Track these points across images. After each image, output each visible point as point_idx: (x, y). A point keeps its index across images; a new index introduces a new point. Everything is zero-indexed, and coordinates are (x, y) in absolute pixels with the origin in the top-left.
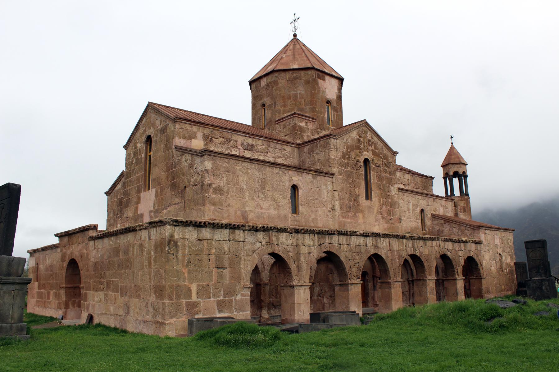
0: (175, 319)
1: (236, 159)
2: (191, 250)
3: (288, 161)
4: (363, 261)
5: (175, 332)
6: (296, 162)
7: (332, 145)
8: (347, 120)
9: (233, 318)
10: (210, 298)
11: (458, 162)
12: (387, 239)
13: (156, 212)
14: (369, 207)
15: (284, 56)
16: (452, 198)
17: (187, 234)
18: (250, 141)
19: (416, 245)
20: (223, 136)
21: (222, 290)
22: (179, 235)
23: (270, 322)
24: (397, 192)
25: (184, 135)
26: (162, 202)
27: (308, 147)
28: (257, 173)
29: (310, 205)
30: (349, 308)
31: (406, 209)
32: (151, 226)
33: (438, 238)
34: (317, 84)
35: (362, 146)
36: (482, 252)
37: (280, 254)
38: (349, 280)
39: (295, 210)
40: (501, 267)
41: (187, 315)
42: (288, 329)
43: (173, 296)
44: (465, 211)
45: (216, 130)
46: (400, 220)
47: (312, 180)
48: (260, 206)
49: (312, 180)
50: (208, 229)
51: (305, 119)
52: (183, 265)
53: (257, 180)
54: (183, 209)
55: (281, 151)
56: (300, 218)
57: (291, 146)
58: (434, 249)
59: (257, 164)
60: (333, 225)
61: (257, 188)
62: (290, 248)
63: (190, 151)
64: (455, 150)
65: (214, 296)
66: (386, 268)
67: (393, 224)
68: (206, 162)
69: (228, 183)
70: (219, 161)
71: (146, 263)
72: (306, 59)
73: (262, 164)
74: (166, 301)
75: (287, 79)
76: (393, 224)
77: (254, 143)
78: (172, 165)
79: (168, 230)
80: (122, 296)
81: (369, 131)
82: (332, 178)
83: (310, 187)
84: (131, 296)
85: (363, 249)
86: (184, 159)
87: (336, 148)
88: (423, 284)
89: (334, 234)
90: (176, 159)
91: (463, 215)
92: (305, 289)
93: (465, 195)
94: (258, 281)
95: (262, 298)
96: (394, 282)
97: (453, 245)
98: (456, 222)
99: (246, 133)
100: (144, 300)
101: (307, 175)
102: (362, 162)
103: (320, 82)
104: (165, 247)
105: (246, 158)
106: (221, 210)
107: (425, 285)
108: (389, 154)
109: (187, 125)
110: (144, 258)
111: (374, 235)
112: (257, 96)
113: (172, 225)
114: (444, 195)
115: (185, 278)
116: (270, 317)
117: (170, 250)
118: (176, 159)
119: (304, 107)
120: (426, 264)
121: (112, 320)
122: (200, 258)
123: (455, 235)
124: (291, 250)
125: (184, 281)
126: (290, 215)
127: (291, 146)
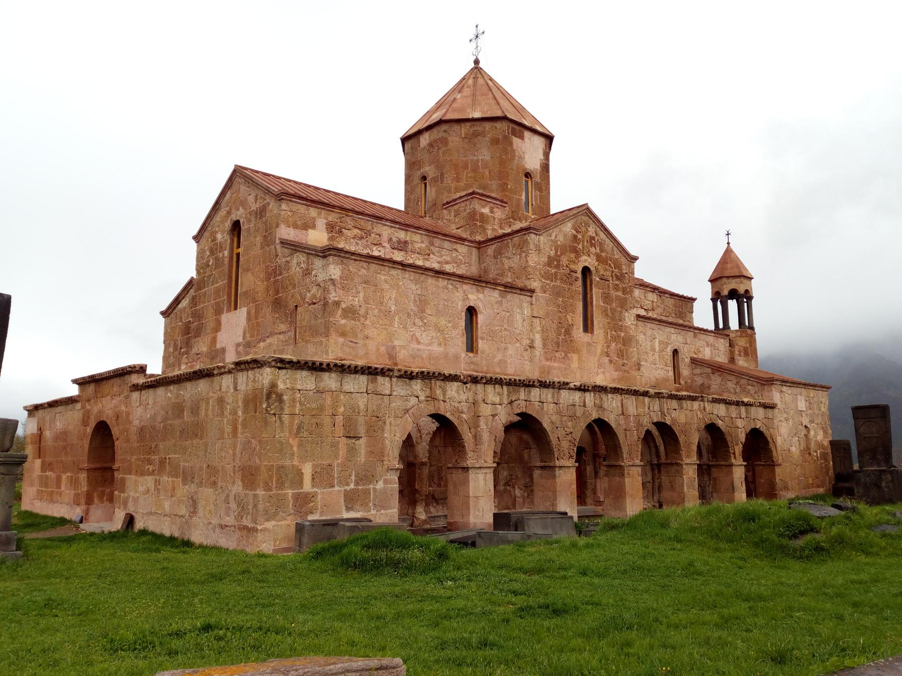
0: (273, 523)
1: (380, 263)
2: (304, 407)
3: (461, 268)
4: (578, 430)
5: (272, 544)
6: (474, 270)
7: (531, 243)
8: (558, 202)
9: (370, 521)
10: (333, 486)
11: (738, 275)
12: (619, 396)
13: (248, 345)
14: (589, 344)
15: (459, 96)
16: (726, 332)
17: (299, 382)
18: (402, 235)
19: (666, 407)
20: (359, 226)
21: (354, 473)
22: (285, 383)
23: (429, 526)
24: (634, 321)
25: (296, 221)
26: (258, 330)
27: (494, 247)
28: (413, 287)
29: (495, 339)
30: (556, 505)
31: (649, 348)
32: (238, 368)
33: (702, 397)
34: (511, 144)
35: (580, 246)
36: (775, 421)
37: (448, 415)
38: (557, 461)
39: (471, 346)
40: (808, 448)
41: (295, 515)
42: (458, 539)
43: (272, 484)
44: (746, 354)
45: (347, 215)
46: (638, 367)
47: (500, 299)
48: (417, 339)
49: (500, 299)
50: (333, 375)
52: (290, 432)
54: (291, 341)
55: (451, 252)
56: (479, 359)
57: (467, 245)
58: (695, 415)
59: (414, 272)
60: (530, 372)
61: (412, 309)
62: (464, 407)
63: (305, 248)
64: (732, 254)
65: (340, 483)
66: (616, 443)
67: (628, 372)
68: (332, 266)
70: (353, 266)
71: (228, 429)
72: (492, 101)
73: (421, 272)
74: (260, 492)
75: (463, 136)
76: (628, 372)
77: (408, 239)
78: (274, 271)
79: (267, 375)
80: (184, 484)
82: (531, 297)
83: (496, 310)
84: (200, 484)
85: (579, 412)
86: (295, 261)
87: (538, 250)
88: (678, 471)
89: (533, 386)
90: (281, 261)
91: (744, 360)
92: (486, 473)
93: (747, 327)
94: (411, 459)
95: (417, 487)
96: (629, 466)
97: (727, 409)
98: (731, 371)
99: (396, 223)
100: (223, 491)
102: (578, 272)
103: (516, 141)
104: (261, 403)
105: (395, 262)
106: (355, 345)
107: (680, 473)
108: (623, 260)
109: (300, 206)
110: (225, 420)
112: (414, 163)
113: (274, 367)
114: (711, 327)
115: (293, 454)
116: (429, 517)
117: (270, 407)
118: (281, 261)
119: (489, 182)
120: (682, 439)
121: (166, 523)
122: (319, 421)
123: (730, 392)
124: (465, 410)
125: (292, 458)
126: (463, 355)
127: (467, 245)
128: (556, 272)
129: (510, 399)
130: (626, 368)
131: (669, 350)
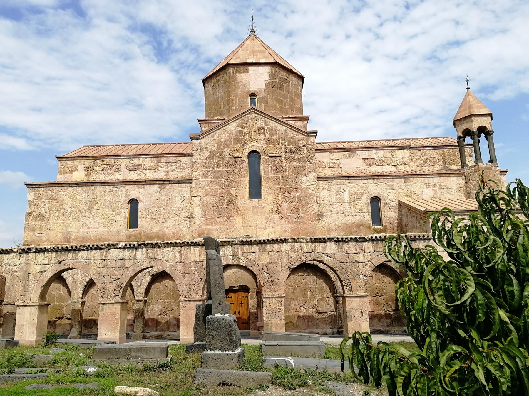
20: (106, 163)
28: (85, 195)
31: (334, 200)
49: (159, 190)
51: (215, 123)
53: (84, 201)
61: (84, 208)
67: (304, 223)
69: (50, 209)
77: (141, 163)
81: (260, 116)
82: (191, 183)
85: (128, 263)
96: (185, 301)
101: (152, 185)
109: (68, 161)
111: (148, 246)
119: (223, 109)
128: (218, 162)
129: (58, 260)
130: (302, 220)
131: (366, 199)
